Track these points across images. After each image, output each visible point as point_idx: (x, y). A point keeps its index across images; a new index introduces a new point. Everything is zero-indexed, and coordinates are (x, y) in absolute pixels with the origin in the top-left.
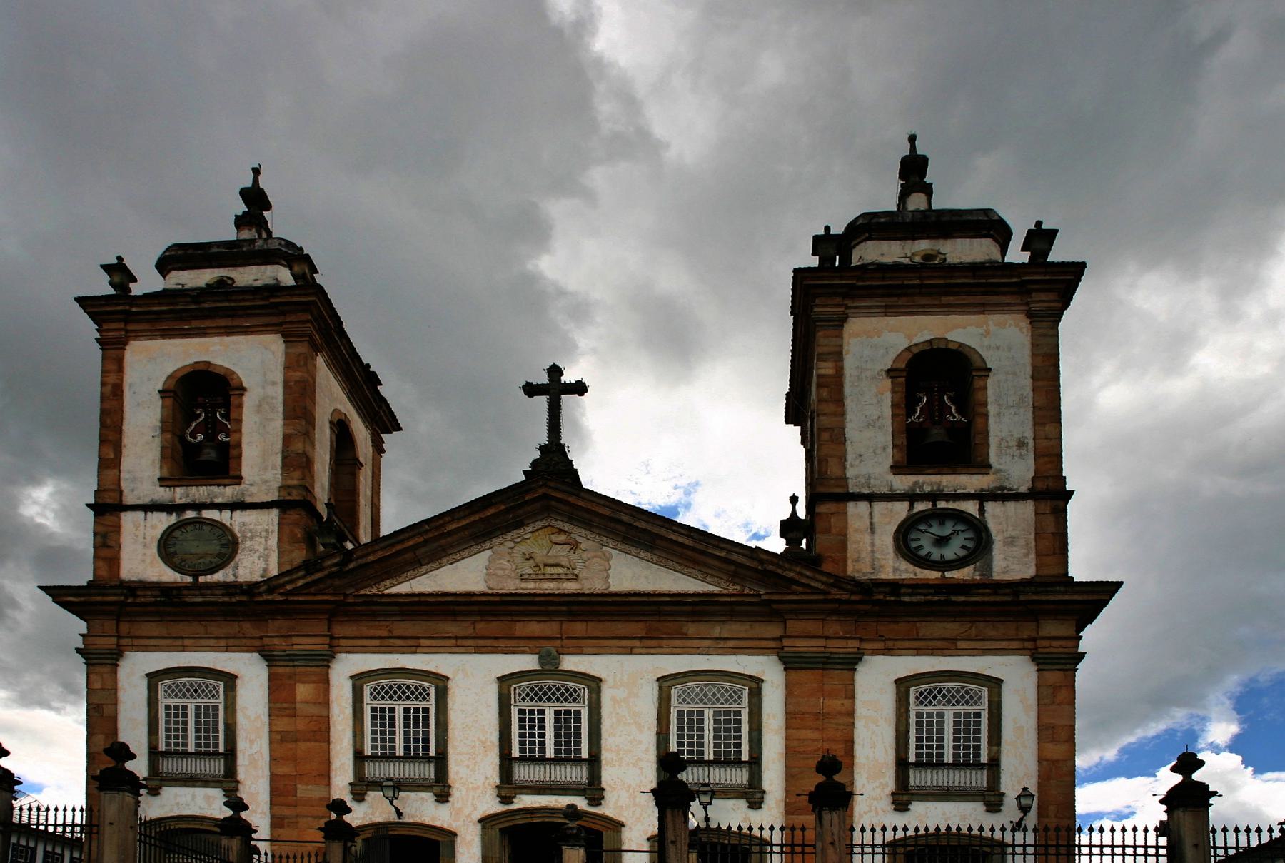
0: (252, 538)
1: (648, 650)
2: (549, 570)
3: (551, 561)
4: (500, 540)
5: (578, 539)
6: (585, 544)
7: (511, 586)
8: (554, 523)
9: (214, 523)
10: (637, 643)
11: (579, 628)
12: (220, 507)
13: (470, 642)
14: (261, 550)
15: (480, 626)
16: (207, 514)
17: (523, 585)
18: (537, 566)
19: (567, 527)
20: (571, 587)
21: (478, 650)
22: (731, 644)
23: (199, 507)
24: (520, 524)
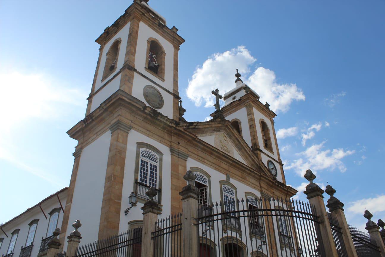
2: (225, 148)
4: (216, 133)
6: (229, 143)
8: (225, 134)
11: (232, 170)
13: (214, 165)
15: (215, 160)
19: (227, 136)
20: (228, 154)
21: (216, 169)
22: (254, 186)
24: (219, 131)
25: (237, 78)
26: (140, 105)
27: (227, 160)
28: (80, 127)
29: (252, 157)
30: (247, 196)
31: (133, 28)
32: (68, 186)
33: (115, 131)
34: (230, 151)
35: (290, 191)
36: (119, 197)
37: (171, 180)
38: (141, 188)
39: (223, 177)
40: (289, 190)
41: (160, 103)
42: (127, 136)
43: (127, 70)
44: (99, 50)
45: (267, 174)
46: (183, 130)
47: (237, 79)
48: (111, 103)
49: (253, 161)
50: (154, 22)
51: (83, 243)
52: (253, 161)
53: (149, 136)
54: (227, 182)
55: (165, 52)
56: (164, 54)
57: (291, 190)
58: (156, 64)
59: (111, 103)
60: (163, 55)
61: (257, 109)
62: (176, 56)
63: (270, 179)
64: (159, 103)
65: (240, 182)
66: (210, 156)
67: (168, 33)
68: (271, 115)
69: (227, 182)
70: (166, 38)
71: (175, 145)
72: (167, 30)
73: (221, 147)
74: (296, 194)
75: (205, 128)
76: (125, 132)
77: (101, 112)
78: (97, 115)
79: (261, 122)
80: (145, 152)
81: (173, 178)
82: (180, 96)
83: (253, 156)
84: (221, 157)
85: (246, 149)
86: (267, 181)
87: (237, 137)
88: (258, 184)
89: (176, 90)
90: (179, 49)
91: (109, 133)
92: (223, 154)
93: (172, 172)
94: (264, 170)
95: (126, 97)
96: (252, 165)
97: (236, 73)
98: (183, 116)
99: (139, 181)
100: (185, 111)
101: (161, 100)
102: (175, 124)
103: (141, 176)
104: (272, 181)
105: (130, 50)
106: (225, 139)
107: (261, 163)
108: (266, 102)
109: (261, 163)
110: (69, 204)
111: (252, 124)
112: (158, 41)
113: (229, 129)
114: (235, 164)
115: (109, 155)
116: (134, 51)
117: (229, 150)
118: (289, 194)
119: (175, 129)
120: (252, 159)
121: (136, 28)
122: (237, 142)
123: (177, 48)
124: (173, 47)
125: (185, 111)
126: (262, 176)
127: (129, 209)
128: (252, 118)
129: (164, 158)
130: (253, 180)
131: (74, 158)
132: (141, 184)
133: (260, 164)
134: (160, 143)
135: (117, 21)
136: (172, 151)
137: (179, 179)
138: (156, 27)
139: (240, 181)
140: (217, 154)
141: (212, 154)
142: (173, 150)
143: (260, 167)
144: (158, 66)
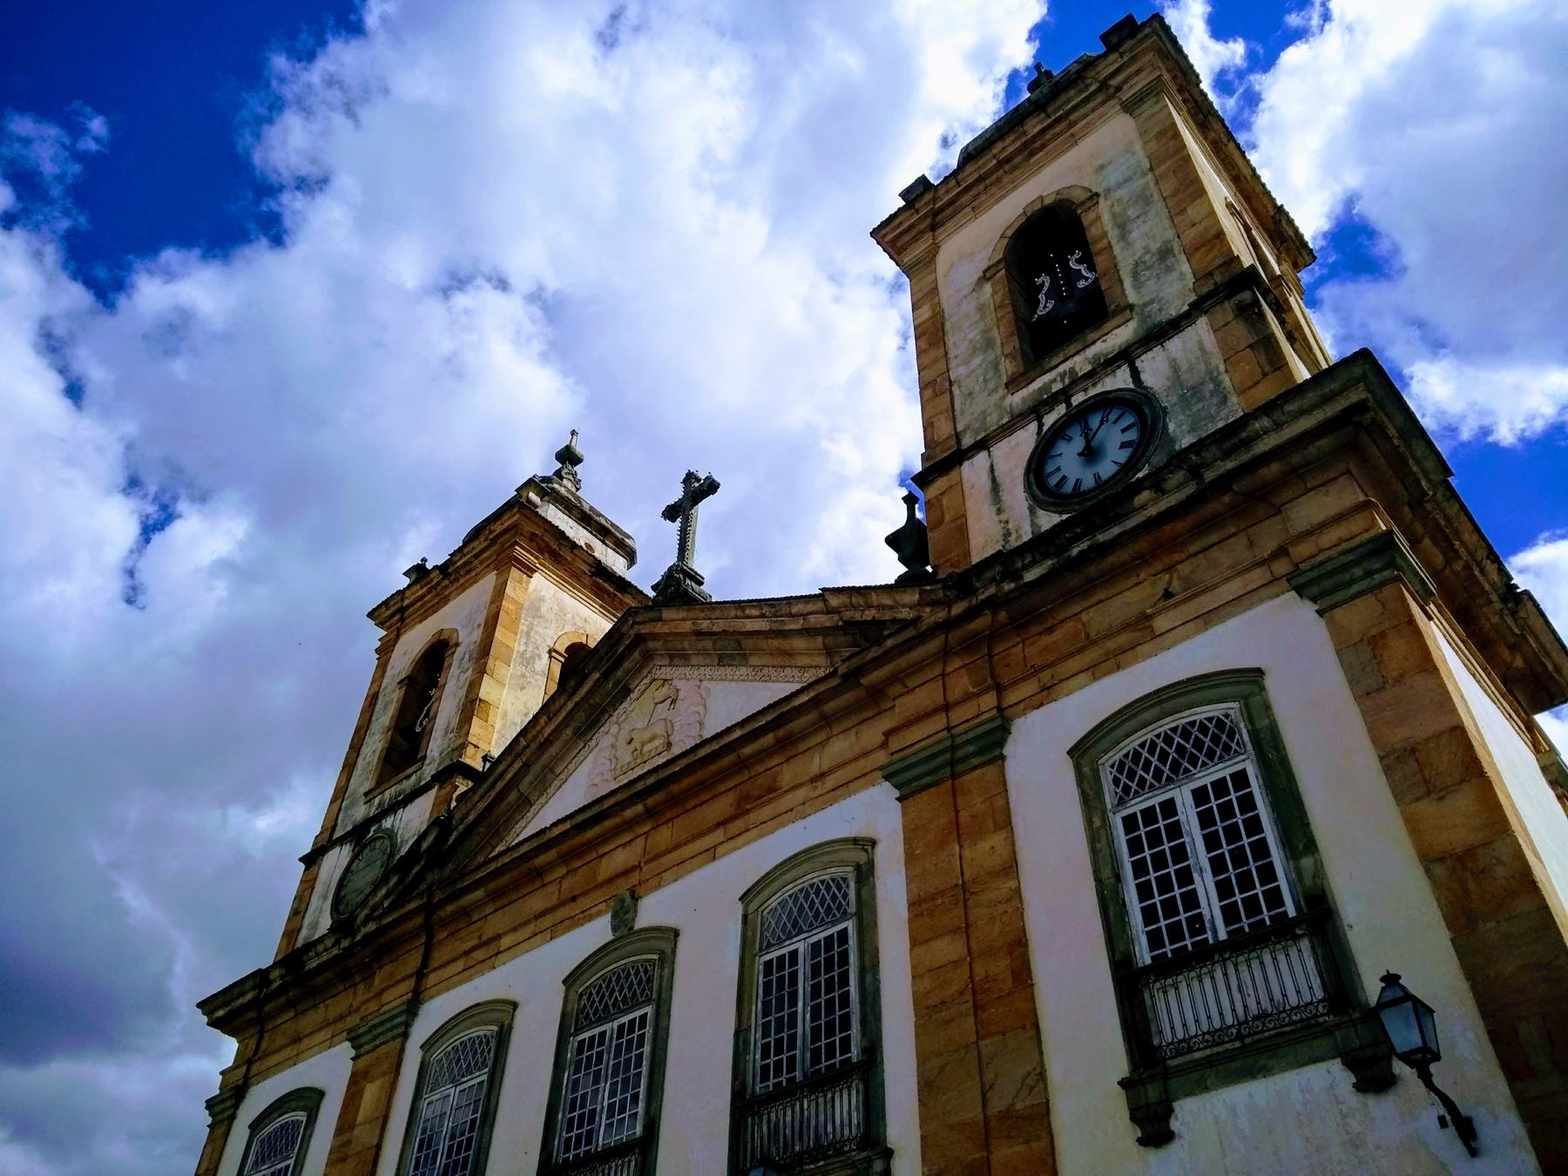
10: (719, 835)
22: (830, 782)
24: (625, 692)
27: (608, 824)
38: (1225, 974)
40: (1209, 475)
57: (1247, 443)
66: (544, 885)
67: (476, 556)
68: (1115, 82)
72: (468, 553)
84: (577, 840)
85: (750, 625)
86: (934, 645)
92: (567, 826)
104: (958, 609)
140: (552, 854)
141: (539, 873)
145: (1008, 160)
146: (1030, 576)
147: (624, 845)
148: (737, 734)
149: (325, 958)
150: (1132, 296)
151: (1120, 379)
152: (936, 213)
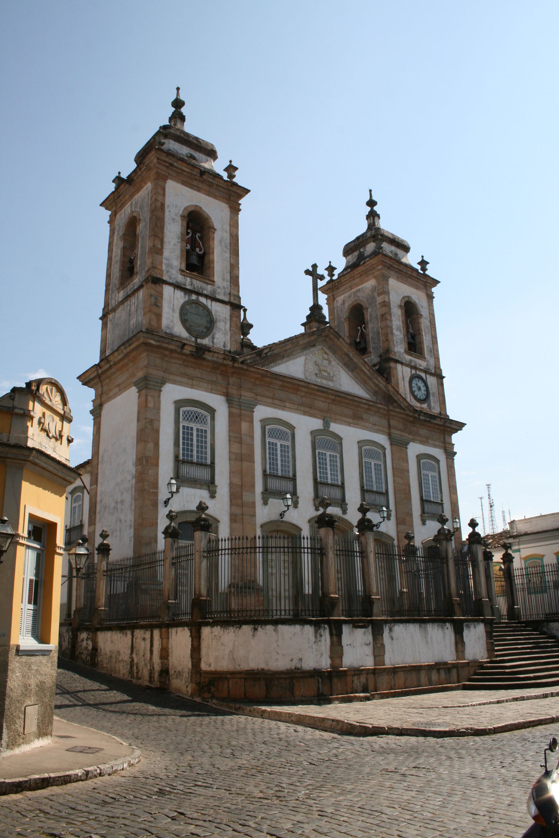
0: (219, 321)
1: (356, 425)
3: (325, 369)
4: (307, 351)
5: (332, 359)
6: (334, 363)
7: (313, 379)
9: (205, 308)
10: (350, 420)
12: (206, 296)
13: (302, 408)
14: (223, 329)
15: (304, 399)
16: (203, 300)
17: (317, 379)
18: (320, 370)
19: (328, 352)
20: (331, 384)
21: (305, 413)
23: (198, 294)
24: (314, 346)
25: (369, 209)
26: (174, 345)
27: (324, 395)
28: (95, 374)
29: (375, 381)
30: (361, 447)
31: (156, 200)
32: (90, 458)
33: (142, 390)
34: (333, 377)
35: (449, 425)
36: (155, 485)
37: (230, 447)
39: (317, 424)
40: (447, 424)
41: (209, 325)
42: (159, 396)
43: (150, 285)
44: (109, 222)
45: (402, 405)
46: (245, 367)
47: (369, 212)
48: (133, 346)
49: (377, 385)
50: (192, 174)
51: (114, 556)
52: (377, 385)
53: (192, 387)
54: (325, 430)
55: (215, 227)
56: (213, 231)
57: (451, 424)
58: (200, 250)
59: (133, 346)
60: (210, 233)
61: (398, 279)
62: (234, 225)
63: (408, 412)
64: (206, 327)
65: (350, 426)
66: (296, 394)
67: (217, 185)
68: (428, 284)
69: (325, 430)
70: (215, 197)
71: (233, 391)
73: (316, 374)
74: (463, 428)
75: (286, 351)
76: (156, 390)
77: (121, 356)
78: (116, 360)
79: (403, 305)
80: (188, 412)
81: (232, 443)
82: (242, 305)
83: (377, 379)
85: (364, 369)
86: (403, 416)
87: (346, 350)
88: (385, 422)
89: (236, 293)
90: (240, 210)
91: (133, 391)
92: (317, 388)
93: (231, 434)
94: (396, 399)
95: (152, 339)
96: (375, 393)
97: (368, 199)
98: (249, 337)
99: (181, 458)
100: (251, 326)
101: (209, 320)
102: (231, 361)
103: (183, 449)
104: (411, 414)
105: (154, 246)
106: (326, 356)
107: (391, 388)
108: (422, 257)
109: (391, 388)
110: (94, 486)
111: (383, 312)
112: (201, 208)
113: (331, 339)
114: (339, 399)
115: (137, 426)
116: (159, 247)
117: (332, 374)
118: (449, 429)
119: (233, 367)
120: (374, 383)
121: (160, 198)
122: (347, 359)
123: (235, 209)
124: (229, 209)
125: (251, 326)
126: (391, 410)
127: (169, 499)
128: (384, 301)
129: (217, 415)
130: (375, 419)
131: (93, 417)
132: (184, 462)
133: (388, 390)
134: (211, 393)
135: (129, 175)
136: (230, 401)
137: (241, 443)
138: (196, 180)
139: (349, 424)
140: (306, 390)
141: (298, 390)
142: (231, 400)
143: (389, 394)
144: (204, 253)
145: (406, 273)
146: (421, 418)
147: (322, 401)
148: (364, 401)
149: (215, 359)
150: (426, 356)
151: (423, 375)
152: (391, 266)
